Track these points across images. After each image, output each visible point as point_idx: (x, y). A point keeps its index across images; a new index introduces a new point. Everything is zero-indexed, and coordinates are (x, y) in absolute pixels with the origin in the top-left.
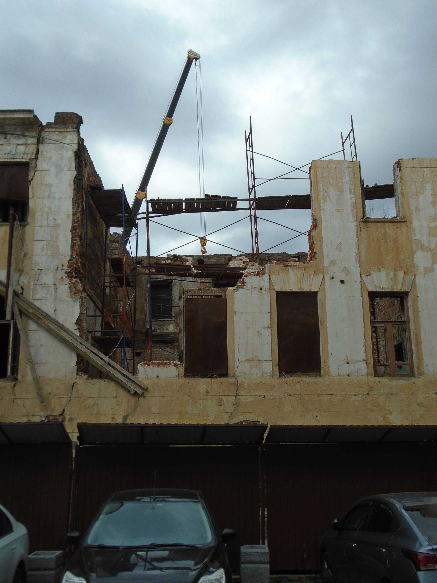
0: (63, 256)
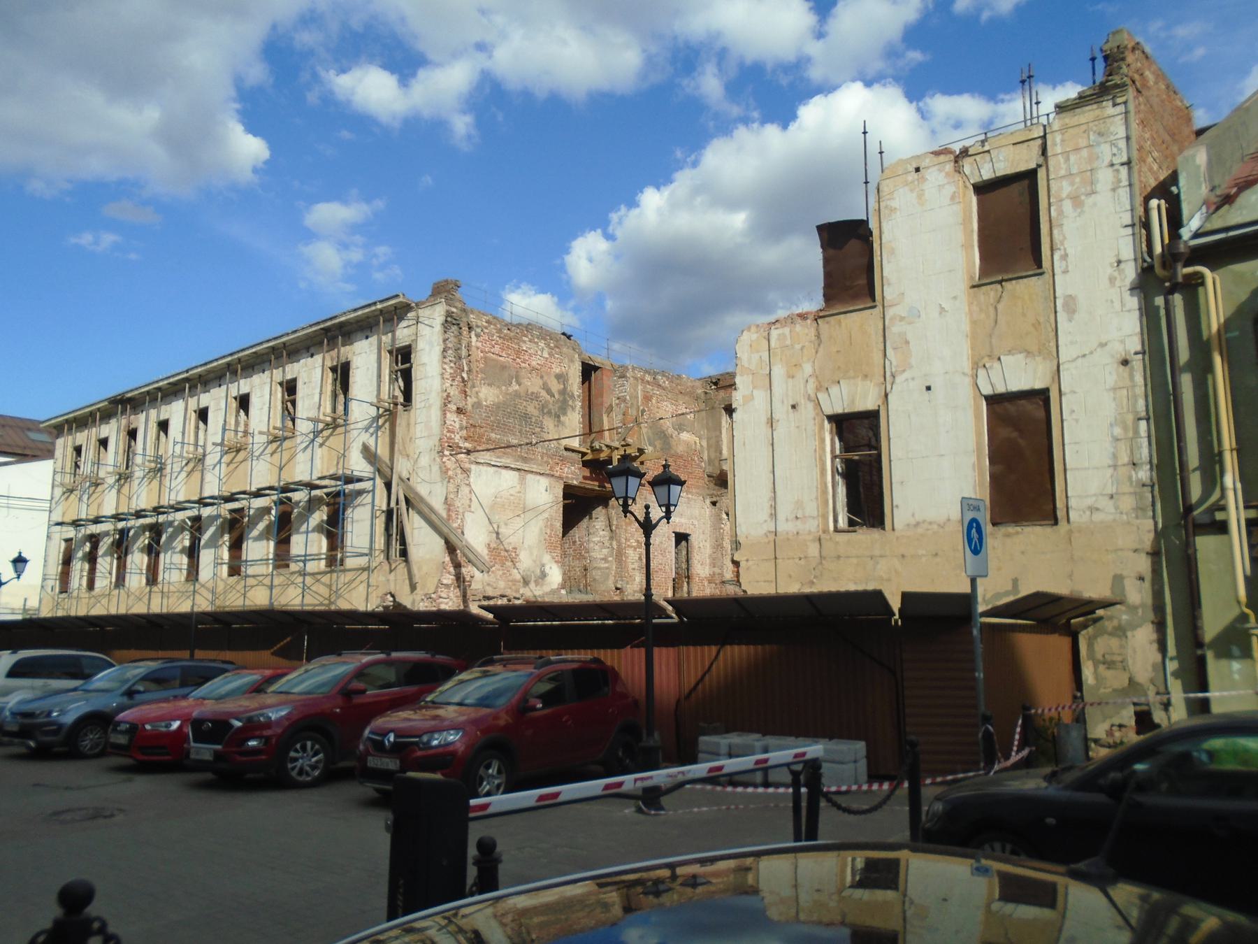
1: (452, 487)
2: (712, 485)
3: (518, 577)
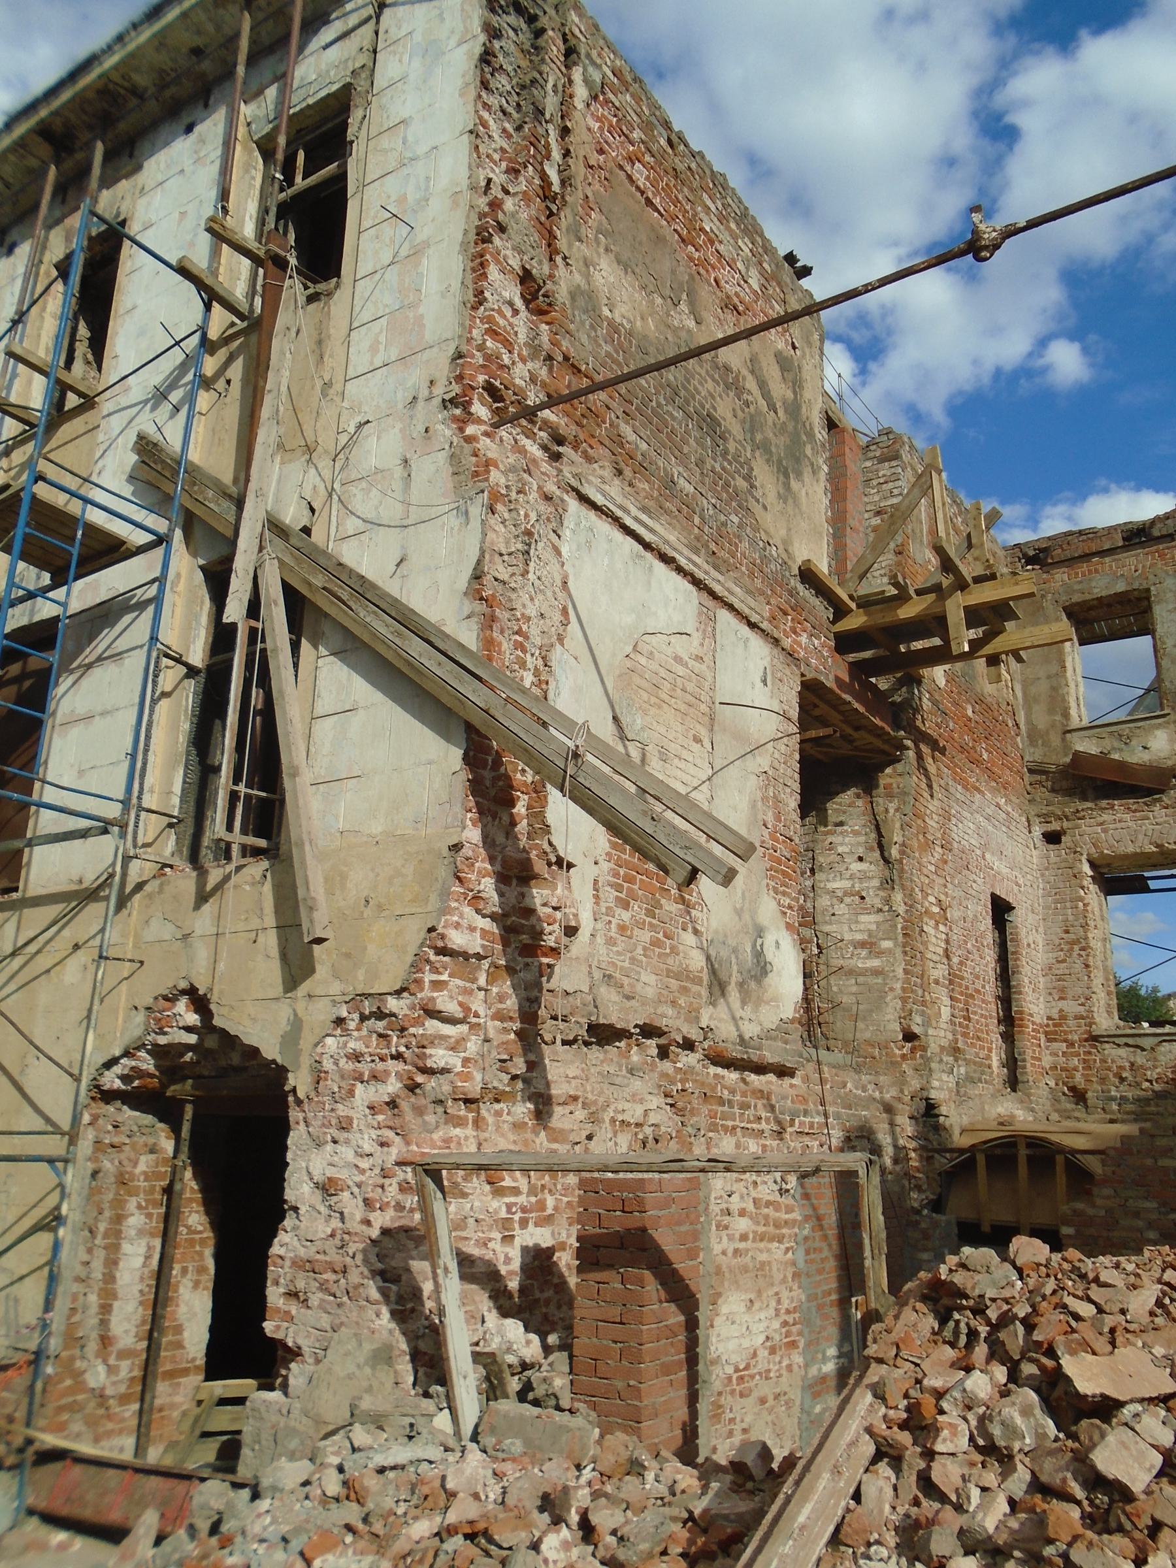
0: (435, 350)
1: (501, 537)
2: (1042, 793)
3: (697, 961)
